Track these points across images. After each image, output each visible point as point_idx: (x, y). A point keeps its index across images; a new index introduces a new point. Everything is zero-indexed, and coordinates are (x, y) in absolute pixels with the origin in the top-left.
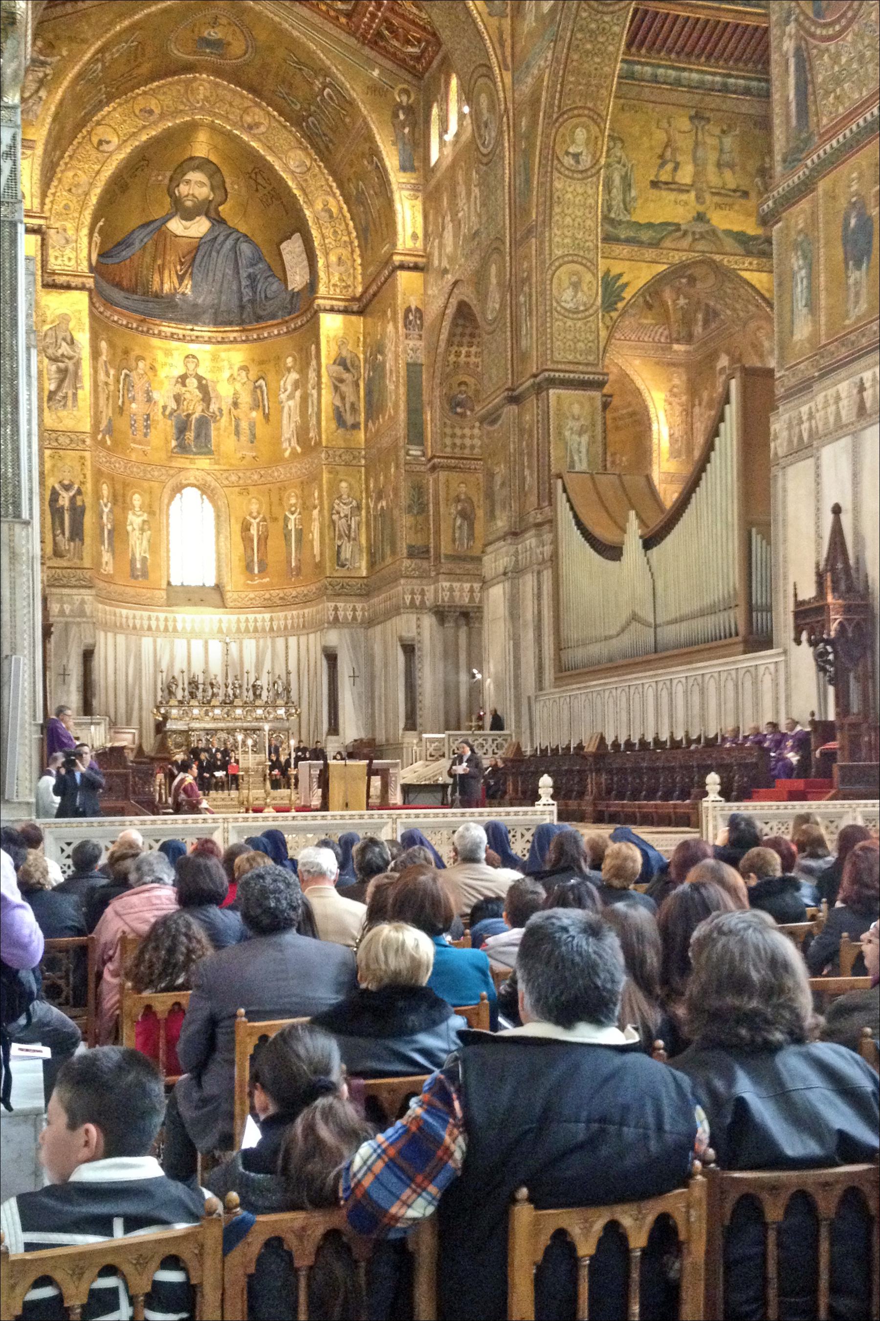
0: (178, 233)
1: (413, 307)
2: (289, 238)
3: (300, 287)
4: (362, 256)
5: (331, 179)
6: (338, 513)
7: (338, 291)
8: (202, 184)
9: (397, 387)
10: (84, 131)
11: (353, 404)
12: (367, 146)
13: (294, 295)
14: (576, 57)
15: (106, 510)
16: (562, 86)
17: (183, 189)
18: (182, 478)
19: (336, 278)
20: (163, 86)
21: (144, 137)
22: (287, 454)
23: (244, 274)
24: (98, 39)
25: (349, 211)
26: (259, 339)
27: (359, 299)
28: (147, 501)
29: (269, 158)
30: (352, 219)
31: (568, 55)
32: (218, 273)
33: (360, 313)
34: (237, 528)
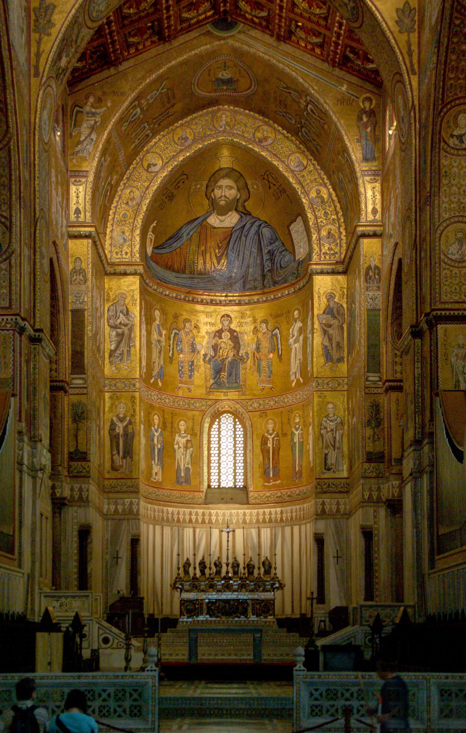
0: (215, 225)
1: (373, 266)
2: (295, 221)
3: (304, 257)
4: (346, 229)
5: (323, 173)
6: (325, 428)
7: (327, 257)
8: (231, 188)
9: (360, 328)
10: (137, 159)
11: (338, 344)
12: (340, 145)
13: (300, 263)
14: (454, 57)
15: (156, 434)
16: (444, 81)
17: (218, 193)
18: (219, 406)
19: (326, 248)
20: (196, 118)
21: (181, 159)
22: (294, 384)
23: (265, 251)
24: (133, 91)
25: (337, 196)
26: (275, 299)
27: (342, 262)
28: (190, 425)
29: (274, 163)
30: (339, 202)
31: (446, 57)
32: (246, 251)
33: (345, 273)
34: (258, 443)
